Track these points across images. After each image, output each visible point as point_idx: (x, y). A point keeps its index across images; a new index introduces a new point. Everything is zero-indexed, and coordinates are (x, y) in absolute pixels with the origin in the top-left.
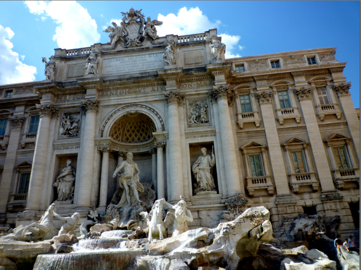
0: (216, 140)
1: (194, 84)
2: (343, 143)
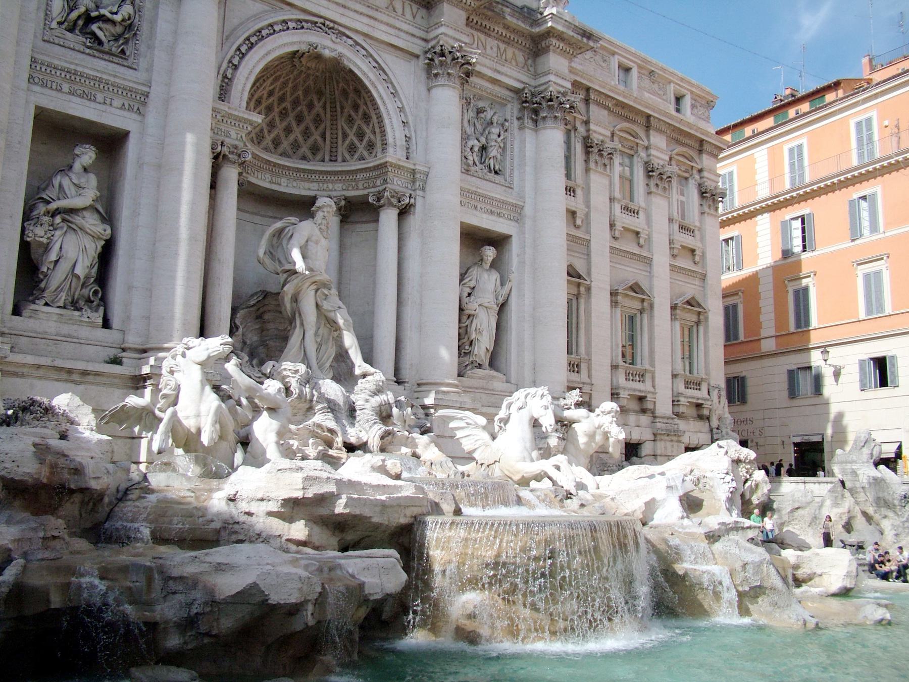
2: (694, 318)
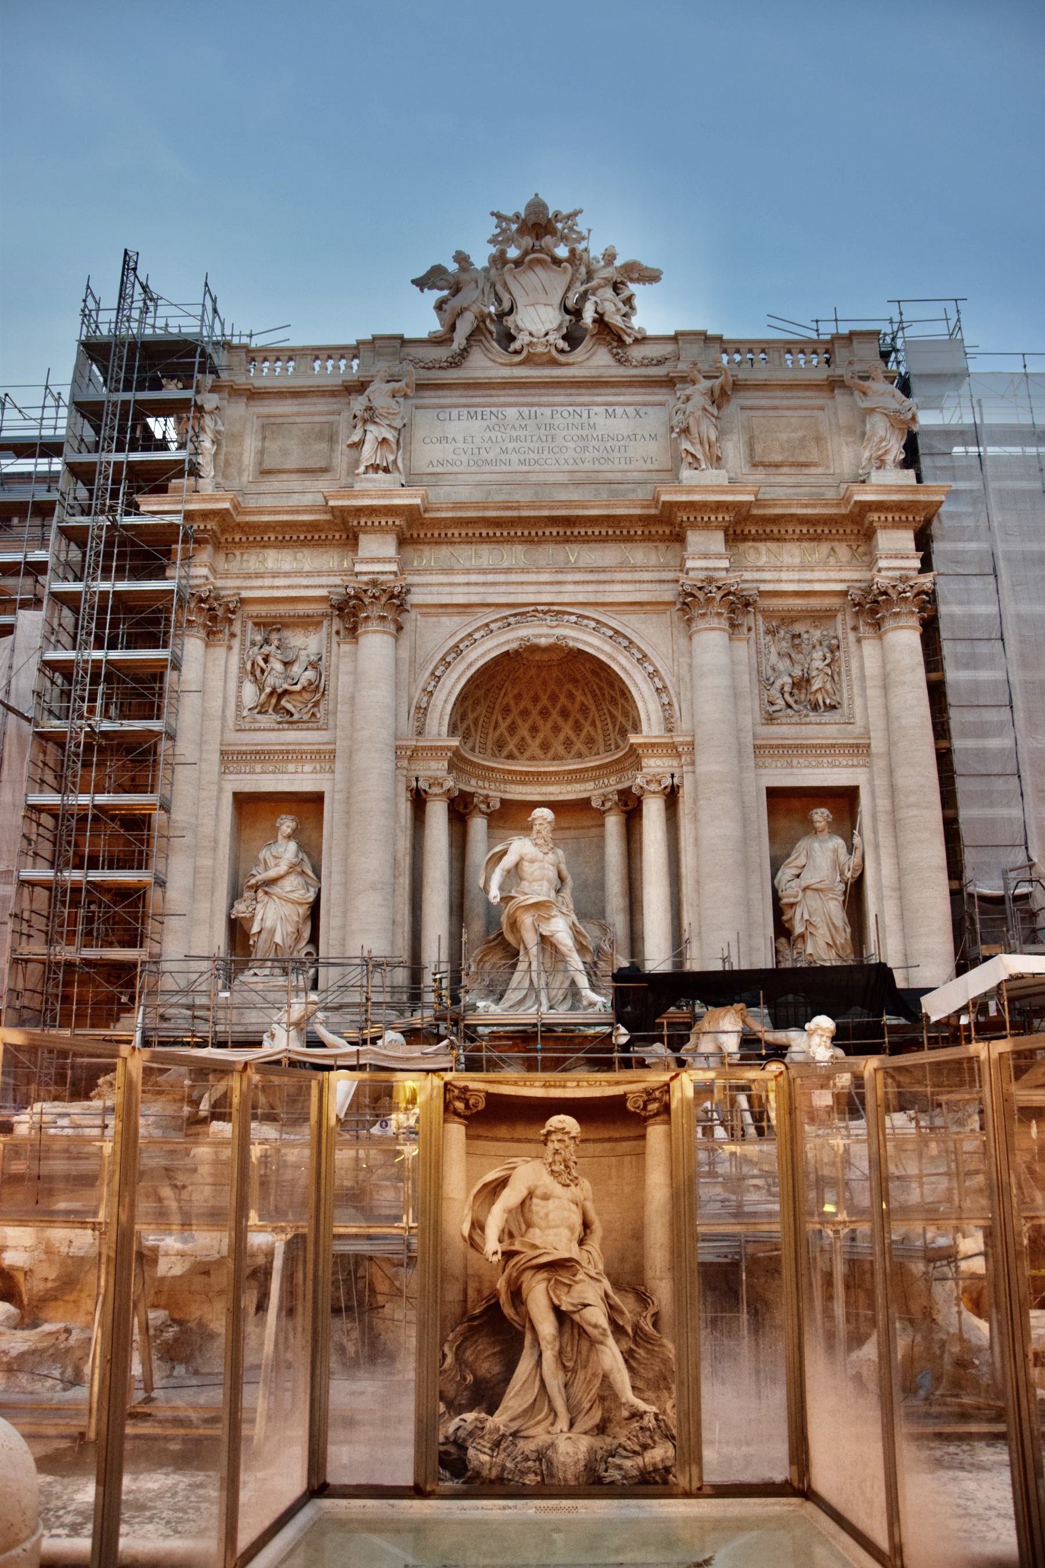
0: (871, 781)
1: (791, 554)
